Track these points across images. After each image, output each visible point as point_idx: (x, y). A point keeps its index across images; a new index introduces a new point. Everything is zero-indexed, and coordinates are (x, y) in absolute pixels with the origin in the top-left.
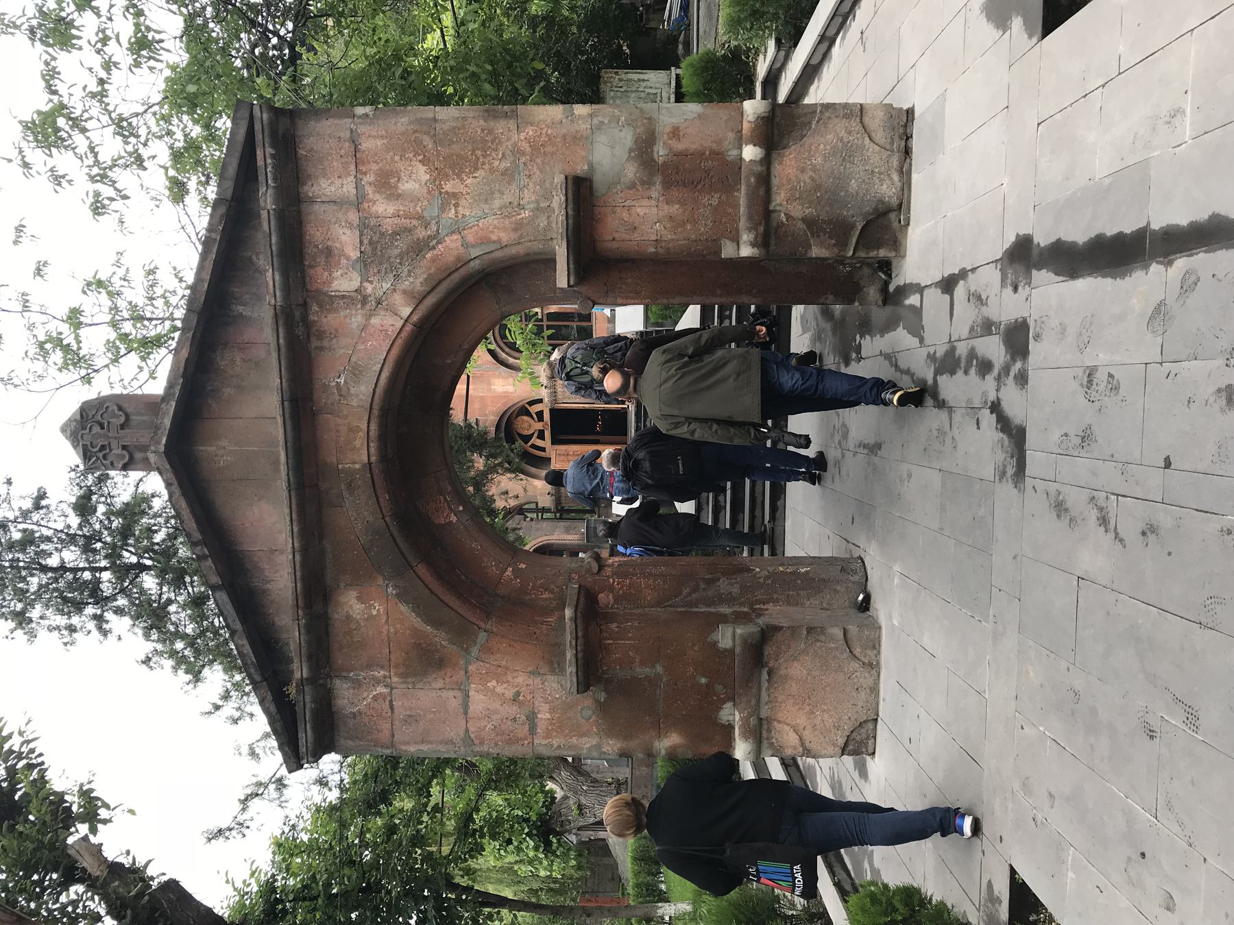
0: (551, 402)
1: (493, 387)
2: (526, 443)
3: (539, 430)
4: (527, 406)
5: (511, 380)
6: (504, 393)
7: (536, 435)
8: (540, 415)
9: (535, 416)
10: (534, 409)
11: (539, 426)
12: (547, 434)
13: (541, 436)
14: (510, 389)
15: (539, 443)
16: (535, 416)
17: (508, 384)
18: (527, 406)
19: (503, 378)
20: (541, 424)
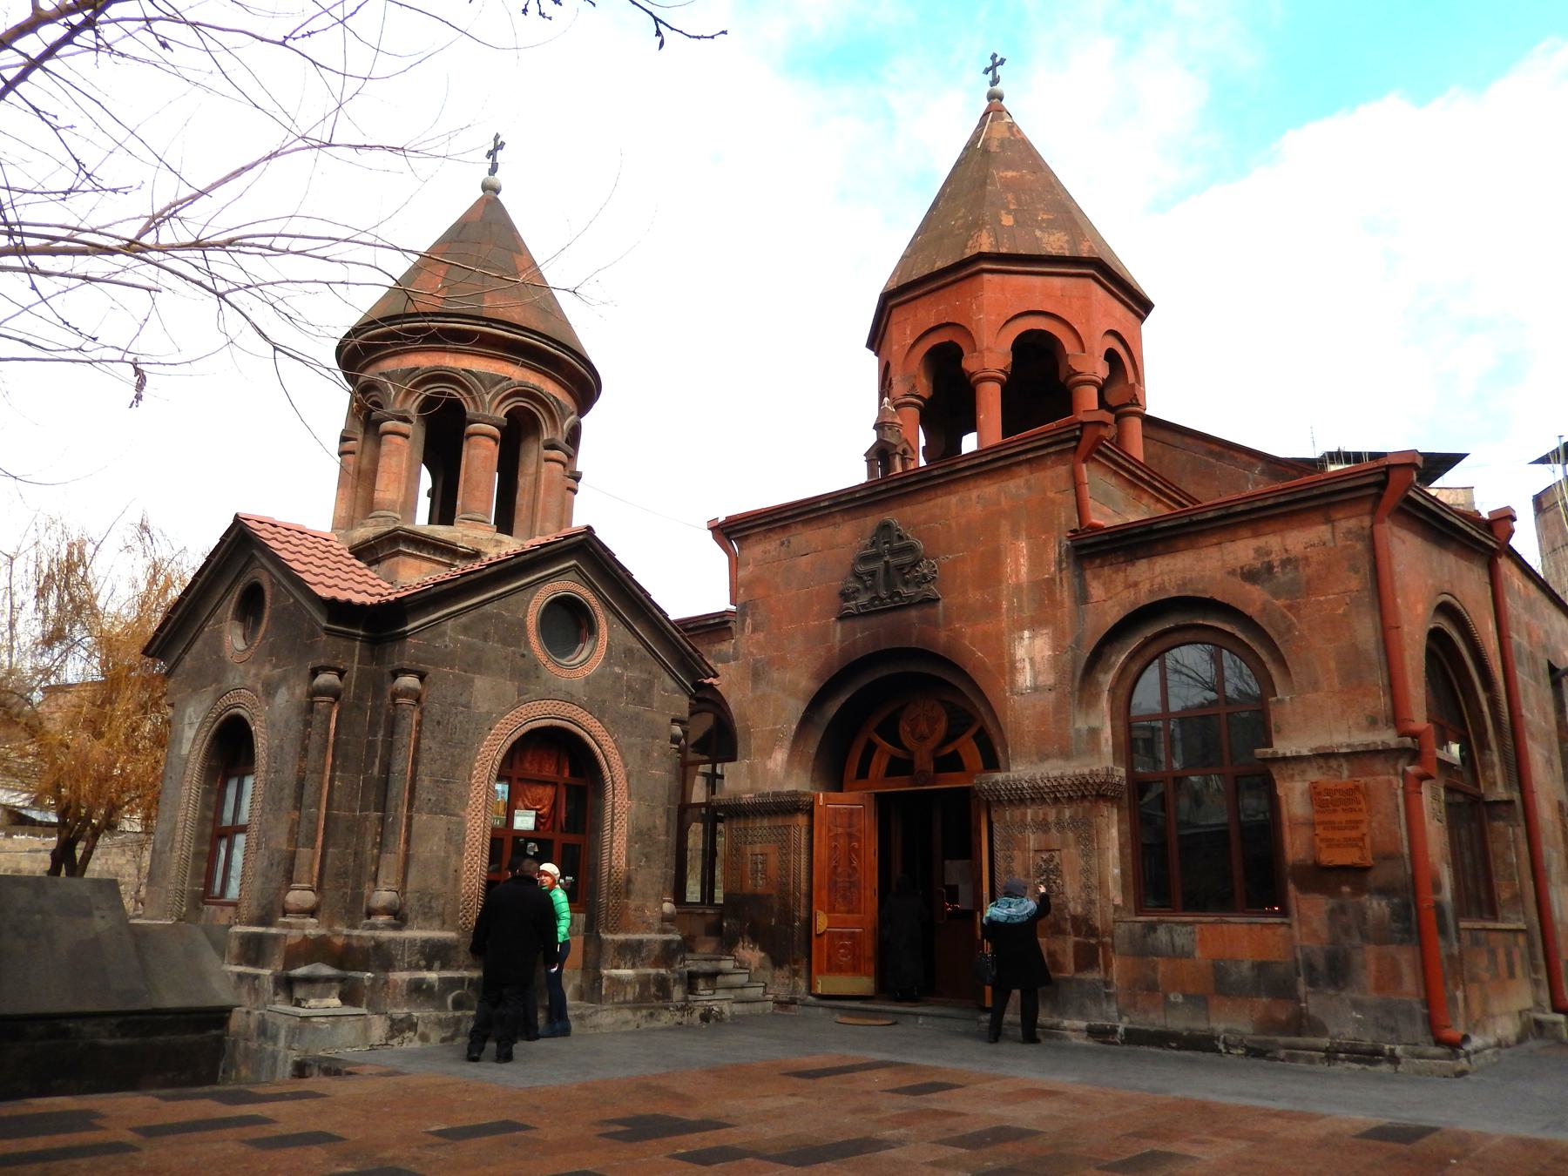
0: (994, 789)
1: (1026, 634)
2: (878, 731)
3: (911, 762)
4: (974, 729)
5: (1048, 679)
6: (1013, 663)
7: (900, 753)
8: (953, 763)
9: (950, 749)
10: (969, 751)
11: (923, 760)
12: (900, 786)
13: (898, 767)
14: (1025, 679)
15: (879, 765)
16: (950, 749)
17: (1035, 677)
18: (974, 729)
19: (1055, 659)
20: (931, 767)
